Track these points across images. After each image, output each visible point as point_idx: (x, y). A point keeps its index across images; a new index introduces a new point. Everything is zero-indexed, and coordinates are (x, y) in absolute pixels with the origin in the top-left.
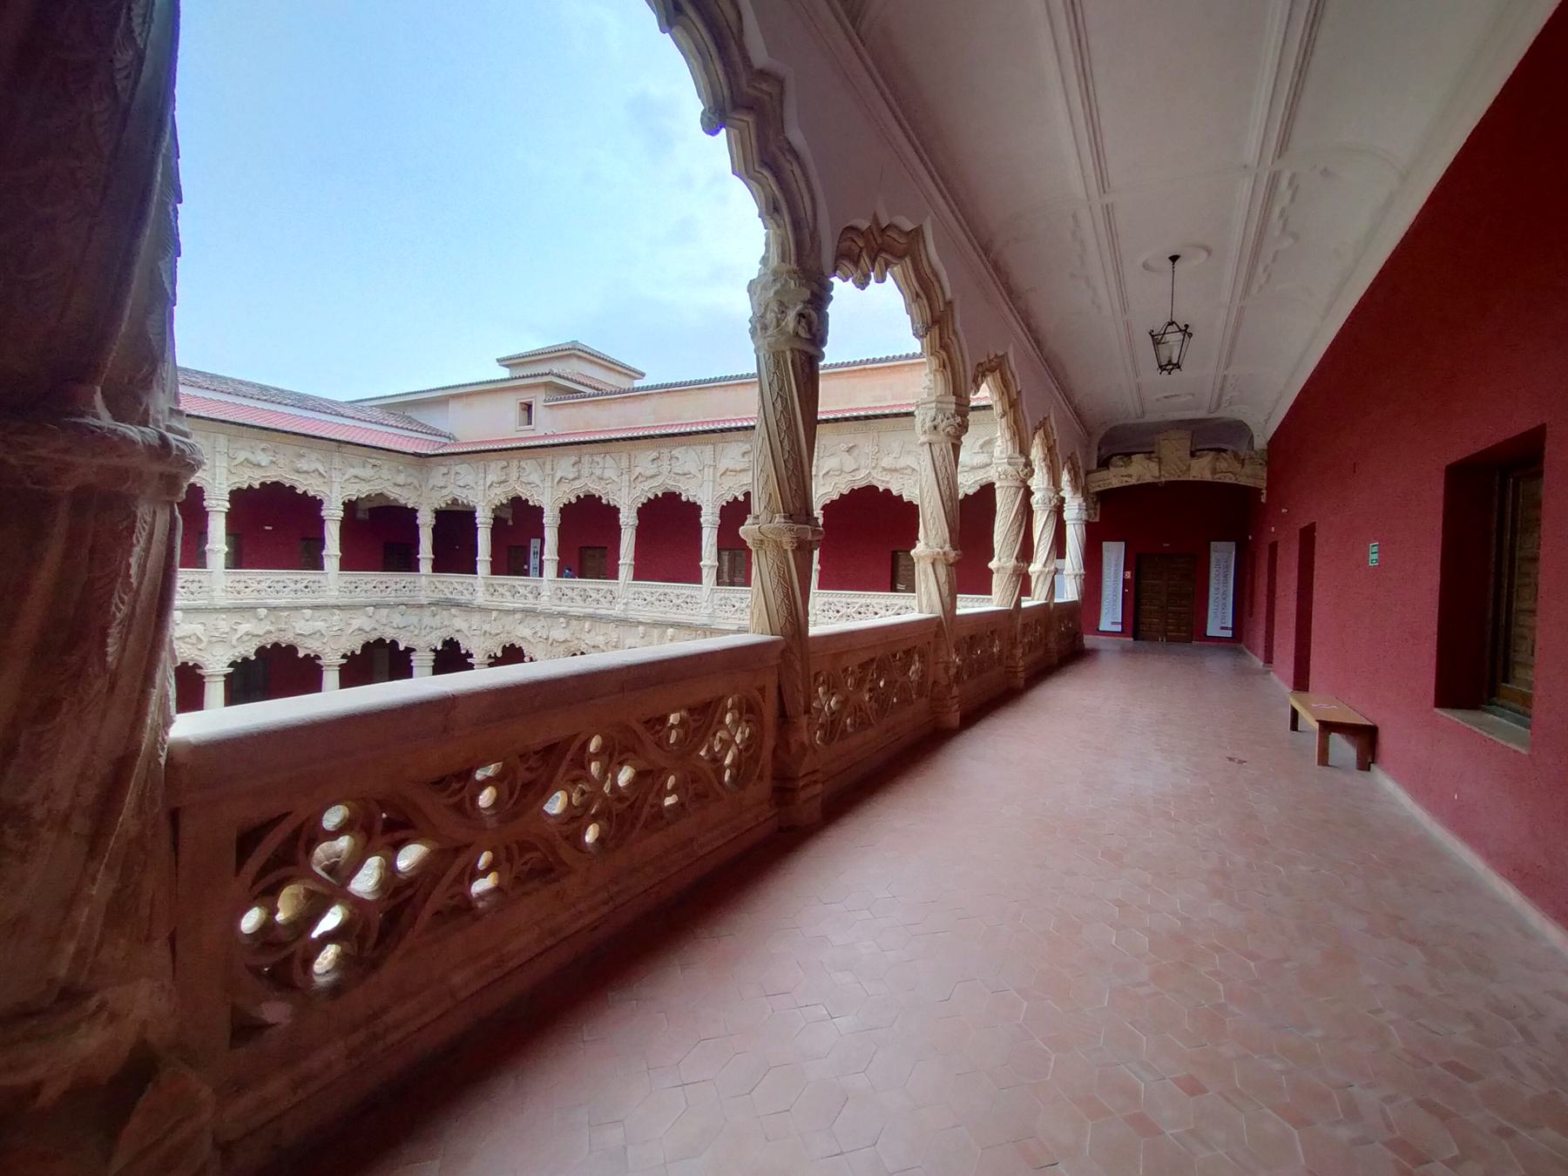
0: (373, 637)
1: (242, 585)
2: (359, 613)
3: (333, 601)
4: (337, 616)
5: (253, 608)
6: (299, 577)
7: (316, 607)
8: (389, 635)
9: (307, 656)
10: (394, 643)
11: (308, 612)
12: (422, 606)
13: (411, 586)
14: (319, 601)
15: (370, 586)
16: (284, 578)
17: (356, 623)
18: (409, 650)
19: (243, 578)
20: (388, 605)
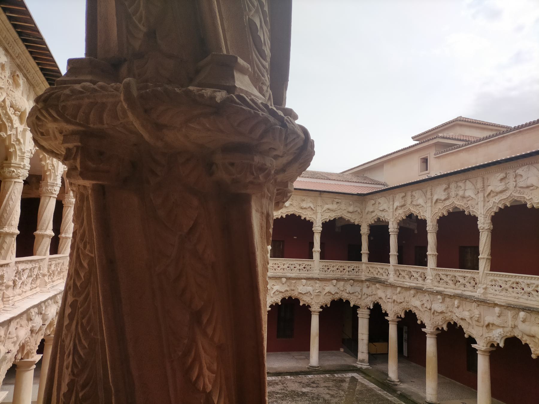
0: (337, 297)
1: (277, 266)
2: (329, 283)
3: (316, 276)
4: (318, 284)
5: (280, 278)
6: (301, 263)
7: (308, 279)
8: (345, 296)
9: (304, 305)
10: (348, 302)
11: (304, 281)
12: (362, 281)
13: (357, 270)
14: (310, 276)
15: (335, 268)
16: (295, 262)
17: (327, 289)
18: (356, 307)
19: (277, 262)
20: (343, 280)
